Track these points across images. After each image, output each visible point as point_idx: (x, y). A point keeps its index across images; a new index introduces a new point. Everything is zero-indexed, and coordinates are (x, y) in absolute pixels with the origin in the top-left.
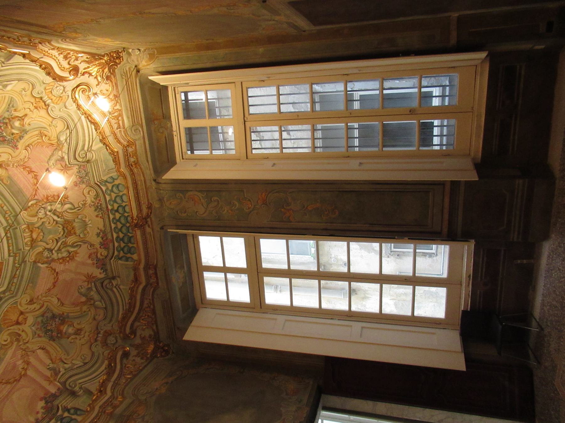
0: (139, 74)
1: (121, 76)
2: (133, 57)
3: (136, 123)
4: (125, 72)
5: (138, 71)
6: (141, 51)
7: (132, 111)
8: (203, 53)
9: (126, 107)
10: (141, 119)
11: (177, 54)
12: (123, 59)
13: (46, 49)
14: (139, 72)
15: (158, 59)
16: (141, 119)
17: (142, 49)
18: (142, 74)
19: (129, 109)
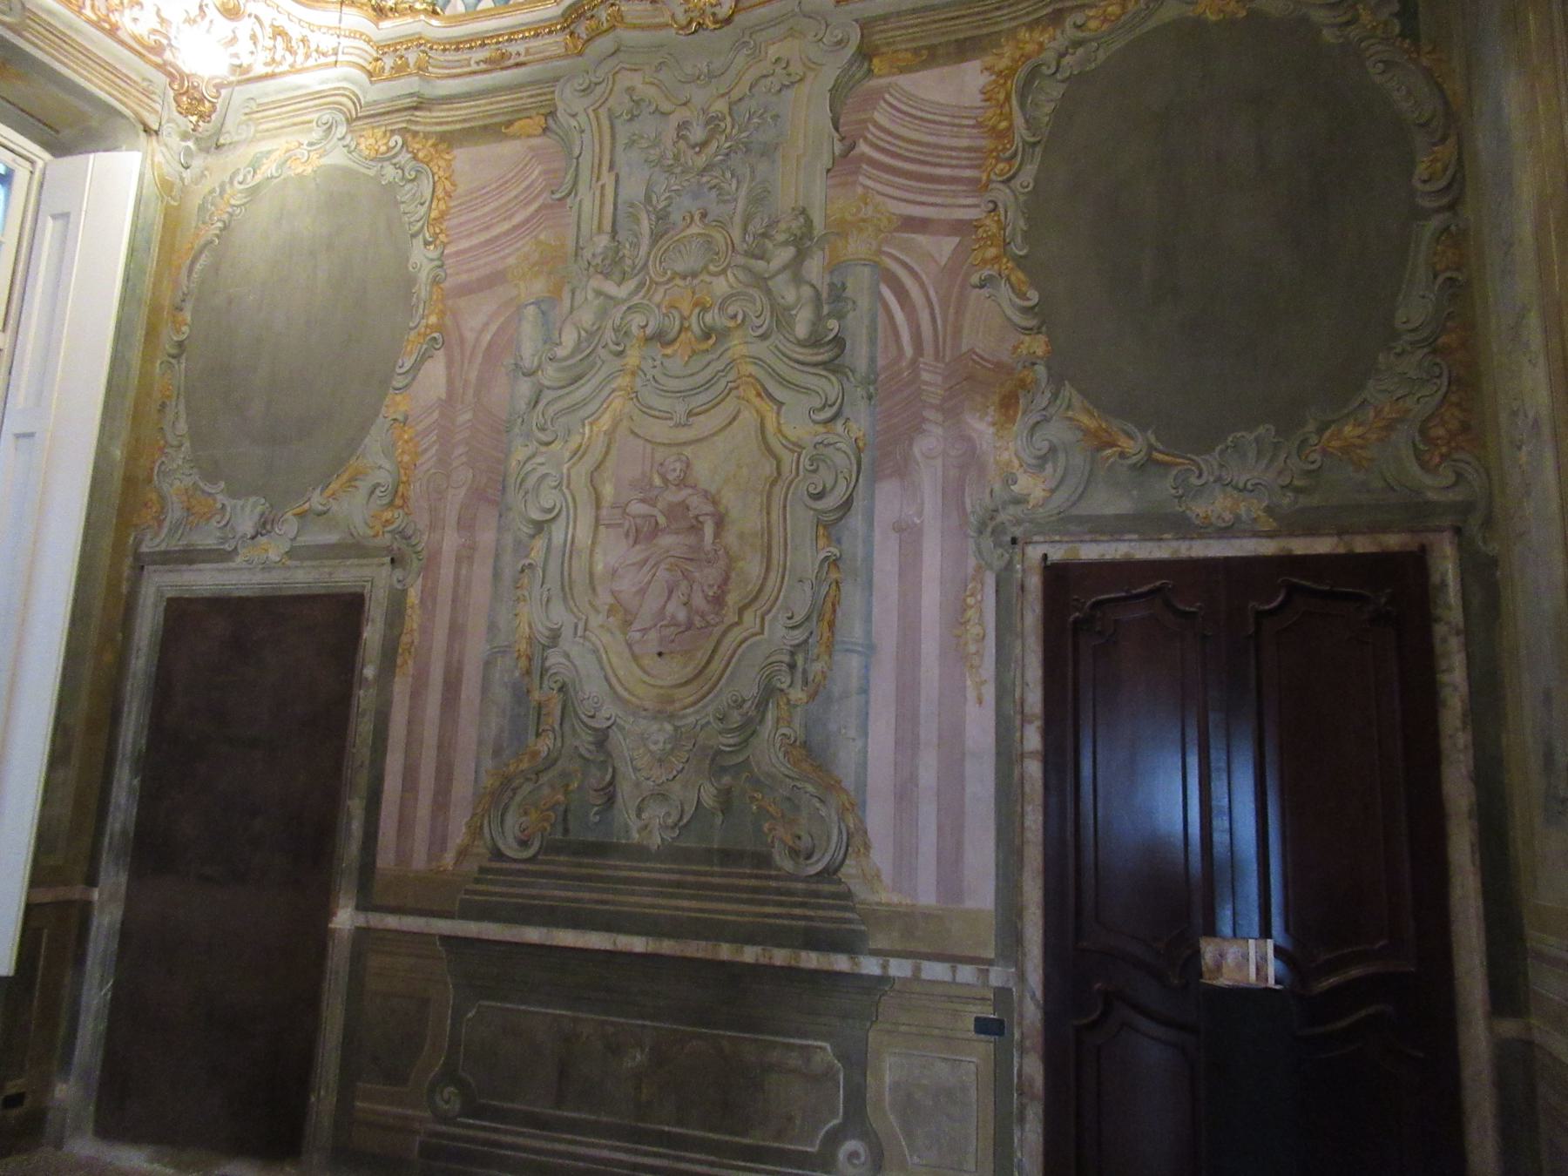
0: (141, 127)
1: (151, 81)
2: (175, 142)
3: (28, 21)
4: (153, 96)
5: (147, 130)
6: (182, 169)
7: (63, 38)
8: (145, 310)
9: (77, 31)
10: (36, 46)
11: (157, 250)
12: (181, 113)
13: (345, 42)
14: (145, 131)
15: (157, 198)
16: (36, 46)
17: (187, 174)
18: (138, 136)
19: (68, 32)
